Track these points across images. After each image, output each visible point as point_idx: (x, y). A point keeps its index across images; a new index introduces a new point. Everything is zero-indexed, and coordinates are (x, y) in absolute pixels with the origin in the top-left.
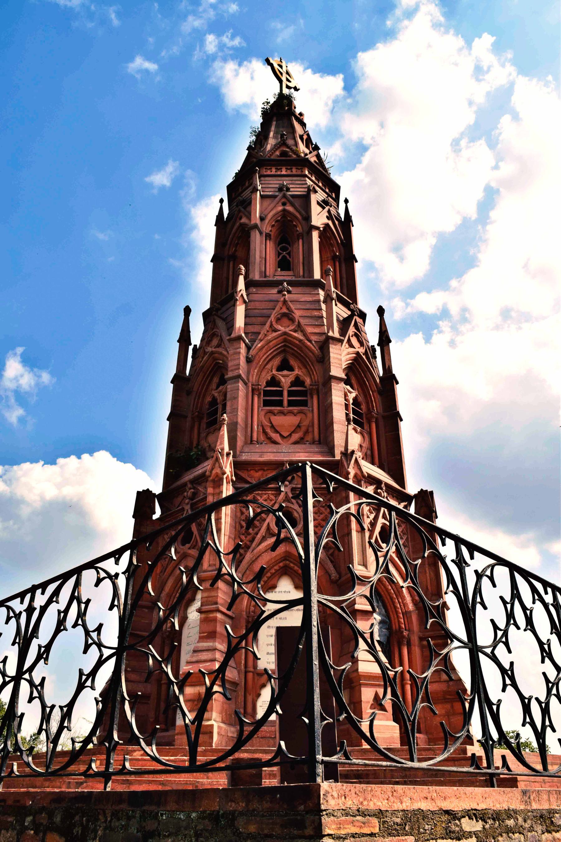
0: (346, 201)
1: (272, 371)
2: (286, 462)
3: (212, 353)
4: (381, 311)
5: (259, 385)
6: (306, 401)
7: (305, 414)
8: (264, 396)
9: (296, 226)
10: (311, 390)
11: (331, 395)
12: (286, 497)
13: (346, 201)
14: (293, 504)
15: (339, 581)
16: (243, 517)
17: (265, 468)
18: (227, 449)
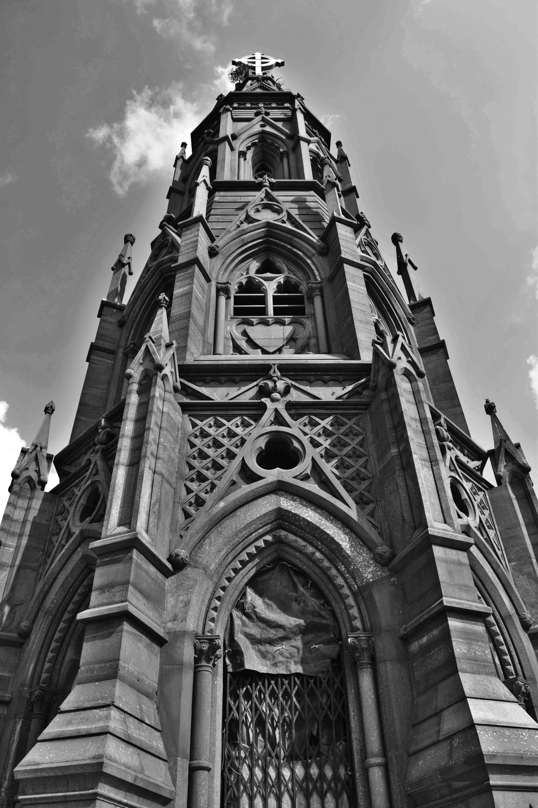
0: (339, 144)
1: (247, 273)
2: (274, 365)
3: (159, 265)
4: (396, 239)
5: (228, 283)
6: (304, 309)
7: (303, 325)
8: (235, 305)
9: (278, 148)
10: (311, 290)
11: (346, 281)
12: (276, 417)
13: (339, 144)
14: (289, 427)
15: (395, 561)
16: (194, 451)
17: (237, 379)
18: (166, 338)
